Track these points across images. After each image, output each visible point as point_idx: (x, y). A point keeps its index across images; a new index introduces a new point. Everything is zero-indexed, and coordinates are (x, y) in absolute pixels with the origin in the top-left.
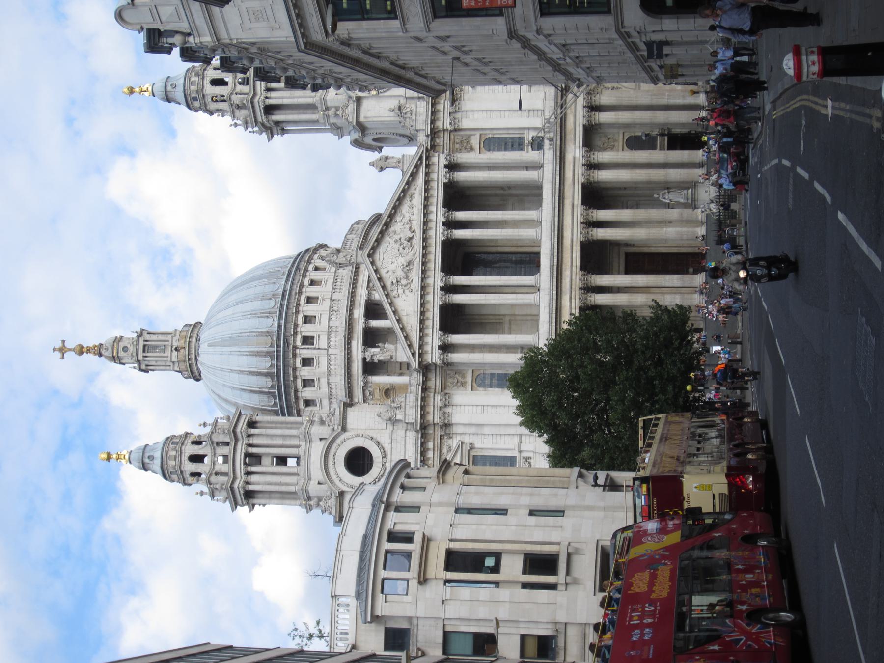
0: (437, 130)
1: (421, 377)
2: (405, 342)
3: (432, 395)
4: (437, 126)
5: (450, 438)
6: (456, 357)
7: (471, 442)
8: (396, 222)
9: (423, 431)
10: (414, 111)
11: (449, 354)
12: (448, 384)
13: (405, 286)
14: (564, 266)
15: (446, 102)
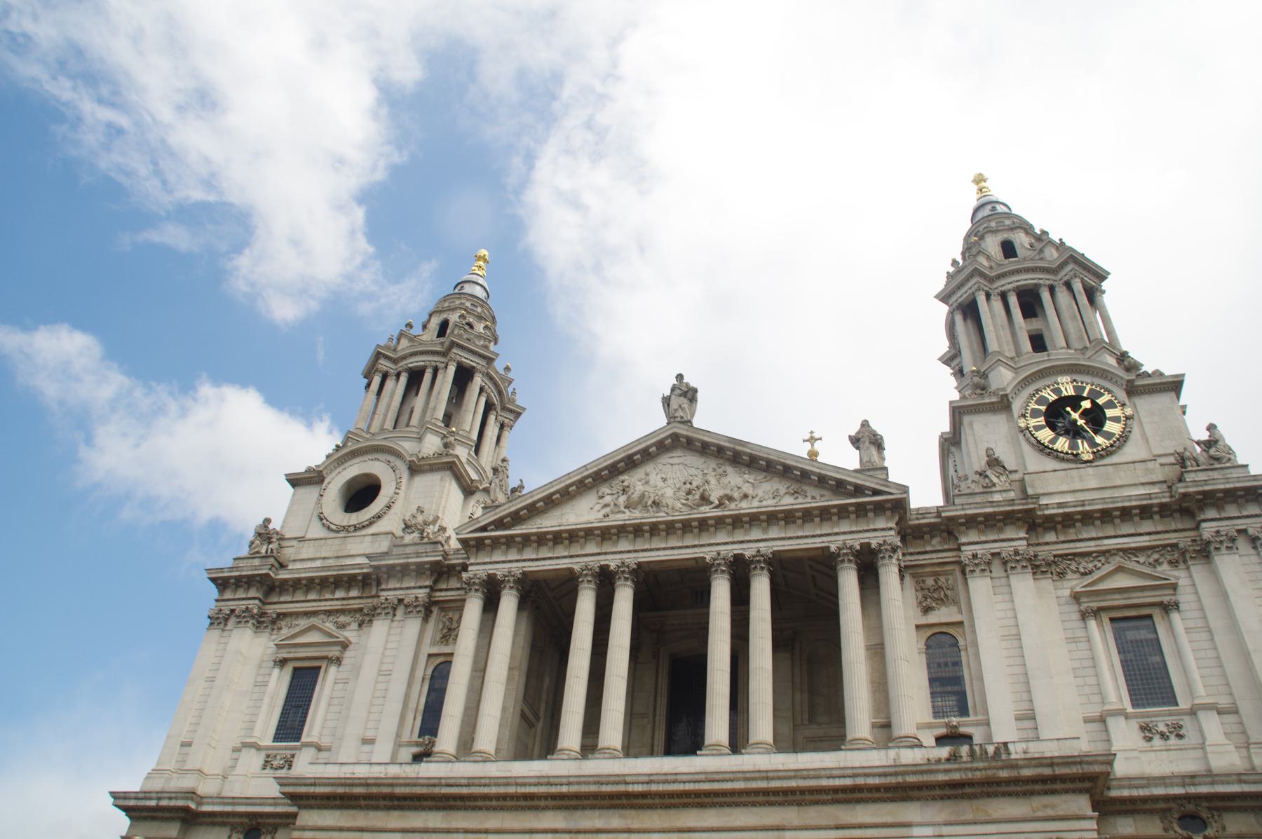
0: (957, 535)
1: (461, 561)
2: (508, 511)
3: (427, 583)
4: (966, 534)
5: (360, 625)
6: (473, 608)
7: (344, 662)
8: (744, 474)
9: (374, 577)
10: (994, 489)
11: (479, 594)
12: (451, 615)
13: (615, 505)
14: (632, 812)
15: (1025, 543)
